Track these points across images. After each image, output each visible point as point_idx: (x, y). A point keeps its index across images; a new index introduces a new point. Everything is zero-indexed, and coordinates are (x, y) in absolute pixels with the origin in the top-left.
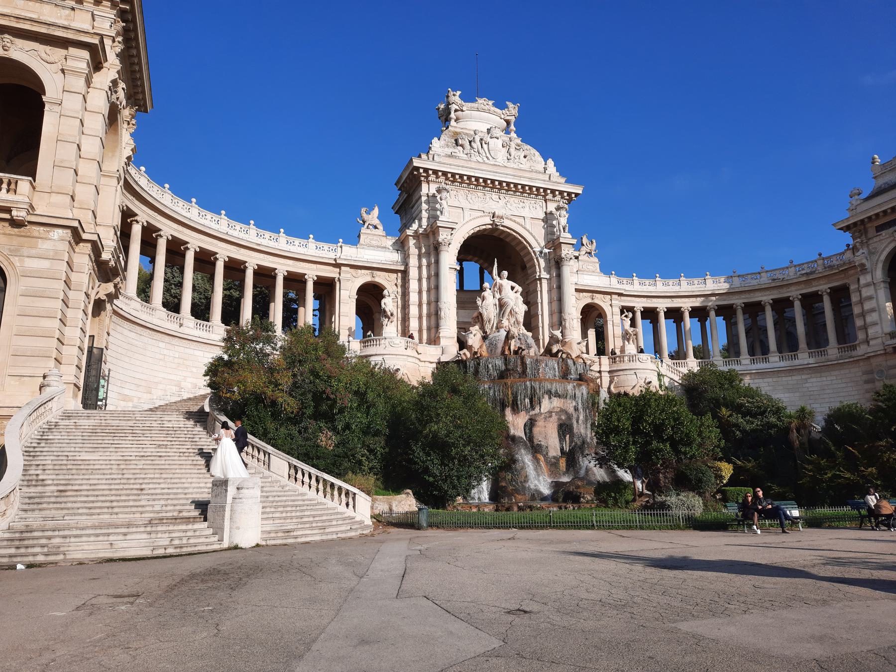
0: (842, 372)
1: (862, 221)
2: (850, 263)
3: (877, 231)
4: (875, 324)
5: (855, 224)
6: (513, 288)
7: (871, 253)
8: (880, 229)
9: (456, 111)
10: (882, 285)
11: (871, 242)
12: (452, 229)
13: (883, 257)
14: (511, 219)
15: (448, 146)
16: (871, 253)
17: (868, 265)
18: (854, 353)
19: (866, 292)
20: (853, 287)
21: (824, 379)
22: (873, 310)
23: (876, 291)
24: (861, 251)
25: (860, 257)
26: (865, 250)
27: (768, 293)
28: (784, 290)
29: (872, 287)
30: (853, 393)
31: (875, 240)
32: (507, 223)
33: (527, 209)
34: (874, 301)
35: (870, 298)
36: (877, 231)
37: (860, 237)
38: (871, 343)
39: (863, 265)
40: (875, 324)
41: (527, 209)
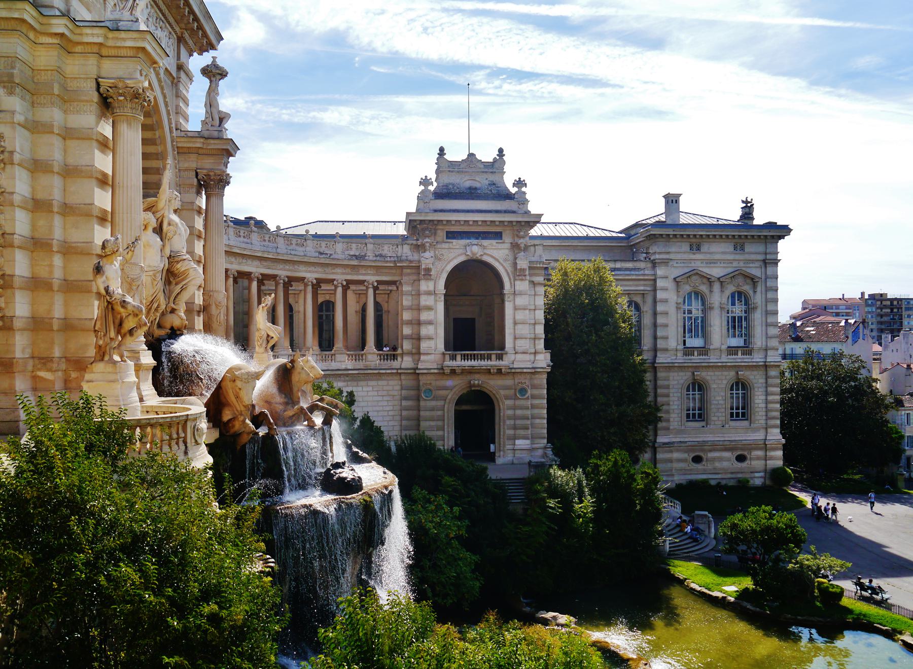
0: (380, 383)
3: (447, 238)
4: (430, 338)
7: (437, 258)
8: (451, 235)
11: (439, 246)
16: (437, 258)
18: (396, 364)
19: (425, 301)
20: (406, 288)
22: (430, 323)
23: (436, 301)
25: (427, 259)
27: (312, 269)
28: (329, 270)
30: (388, 408)
31: (444, 245)
34: (432, 313)
35: (429, 308)
36: (447, 238)
39: (428, 270)
40: (430, 338)
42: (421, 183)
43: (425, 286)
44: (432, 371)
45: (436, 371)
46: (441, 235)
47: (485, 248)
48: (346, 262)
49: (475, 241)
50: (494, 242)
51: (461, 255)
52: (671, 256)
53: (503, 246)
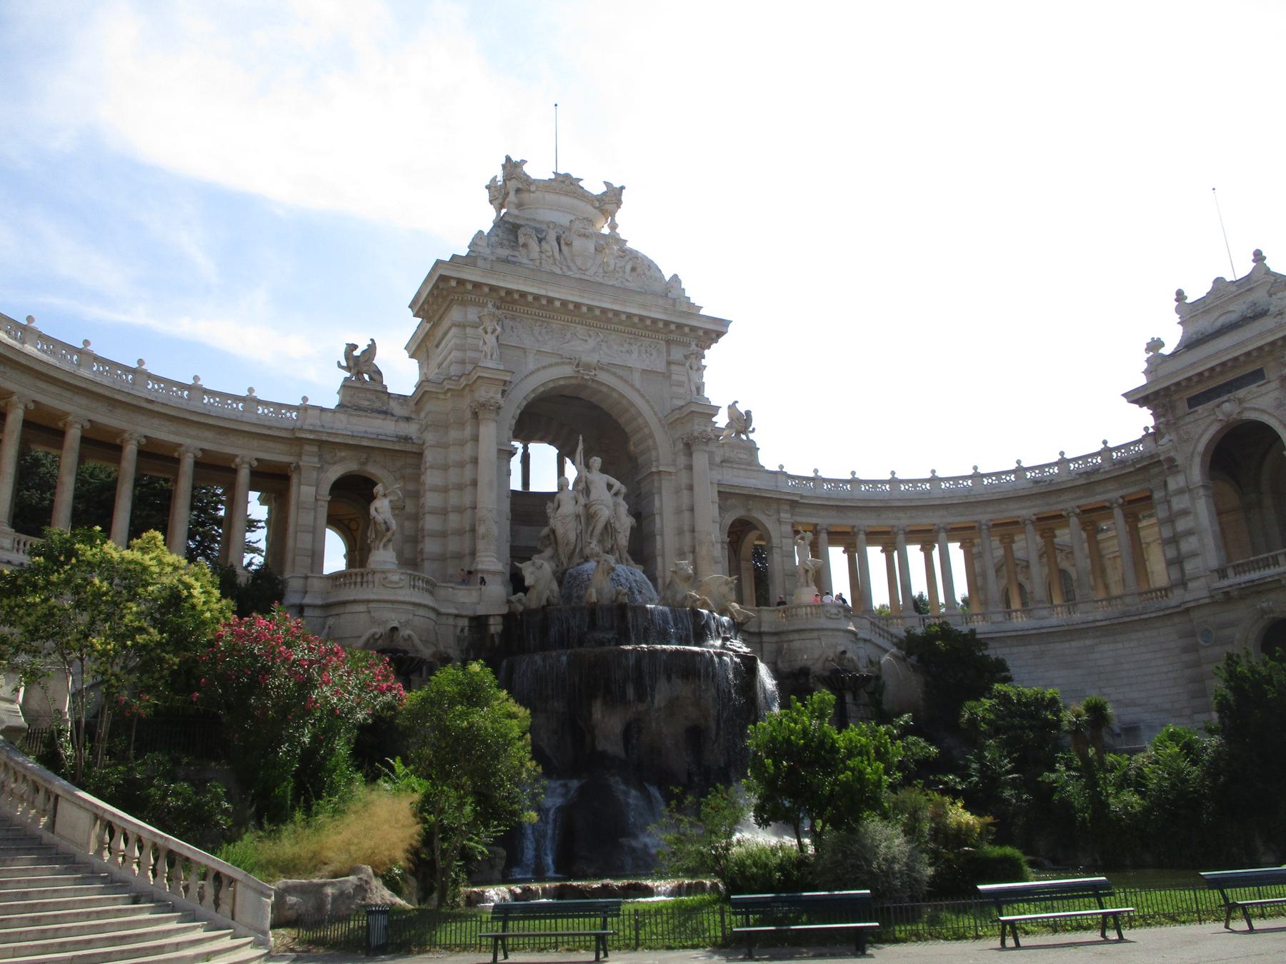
1: (1167, 388)
2: (1152, 457)
3: (1190, 407)
4: (1194, 555)
5: (1157, 393)
6: (610, 487)
8: (1194, 402)
9: (518, 191)
10: (1202, 492)
11: (1181, 422)
12: (505, 382)
13: (1201, 447)
14: (608, 371)
15: (501, 245)
17: (1180, 460)
19: (1178, 503)
20: (1158, 495)
21: (1120, 645)
22: (1190, 533)
24: (1167, 438)
26: (1173, 436)
29: (1187, 496)
31: (1187, 419)
32: (603, 377)
33: (635, 355)
34: (1191, 518)
35: (1185, 513)
36: (1190, 407)
37: (1164, 416)
38: (1190, 585)
39: (1171, 460)
40: (1194, 555)
41: (635, 355)
42: (1147, 350)
43: (1174, 483)
44: (1202, 602)
45: (1207, 601)
46: (1182, 406)
47: (1241, 401)
48: (1070, 484)
49: (1225, 398)
50: (1253, 387)
51: (1211, 424)
53: (1273, 385)
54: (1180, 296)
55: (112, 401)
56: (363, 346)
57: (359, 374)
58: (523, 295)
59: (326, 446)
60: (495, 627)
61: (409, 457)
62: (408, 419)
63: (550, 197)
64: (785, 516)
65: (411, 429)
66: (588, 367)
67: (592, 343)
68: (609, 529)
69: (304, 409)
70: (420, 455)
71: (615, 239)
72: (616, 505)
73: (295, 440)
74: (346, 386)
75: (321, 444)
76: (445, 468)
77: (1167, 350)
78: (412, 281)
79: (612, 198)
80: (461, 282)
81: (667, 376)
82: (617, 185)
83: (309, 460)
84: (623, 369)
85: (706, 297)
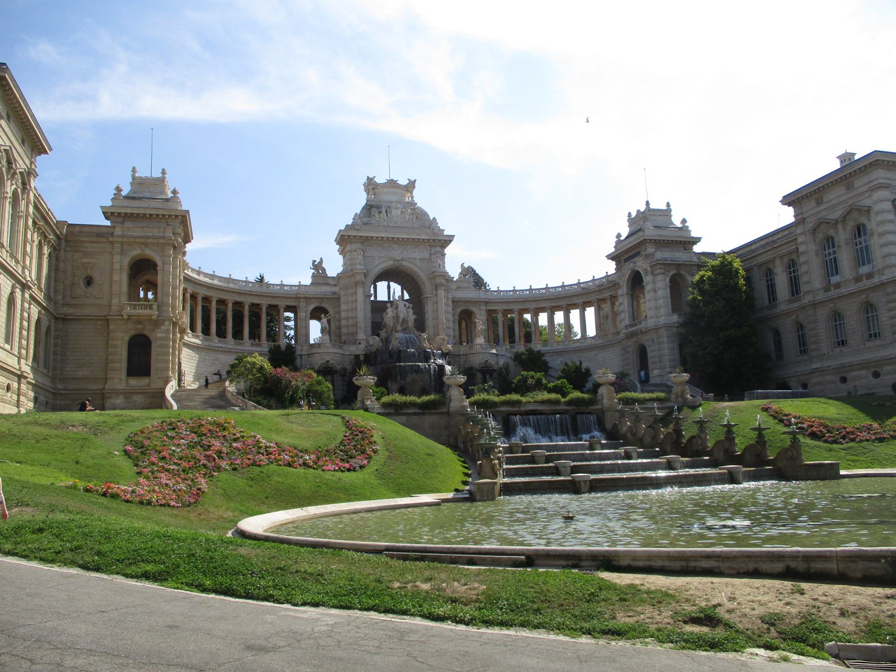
8: (626, 260)
32: (404, 263)
52: (805, 216)
54: (630, 214)
55: (239, 293)
56: (318, 260)
57: (318, 271)
58: (372, 237)
59: (307, 299)
60: (362, 358)
61: (336, 299)
62: (335, 285)
63: (386, 190)
64: (483, 307)
65: (336, 289)
66: (398, 261)
67: (400, 251)
68: (405, 321)
69: (300, 286)
70: (339, 298)
71: (413, 204)
72: (407, 312)
73: (297, 298)
74: (313, 276)
75: (306, 298)
76: (347, 303)
77: (622, 238)
78: (335, 234)
79: (411, 186)
80: (349, 236)
81: (430, 259)
82: (413, 180)
83: (302, 304)
84: (413, 259)
85: (447, 226)
